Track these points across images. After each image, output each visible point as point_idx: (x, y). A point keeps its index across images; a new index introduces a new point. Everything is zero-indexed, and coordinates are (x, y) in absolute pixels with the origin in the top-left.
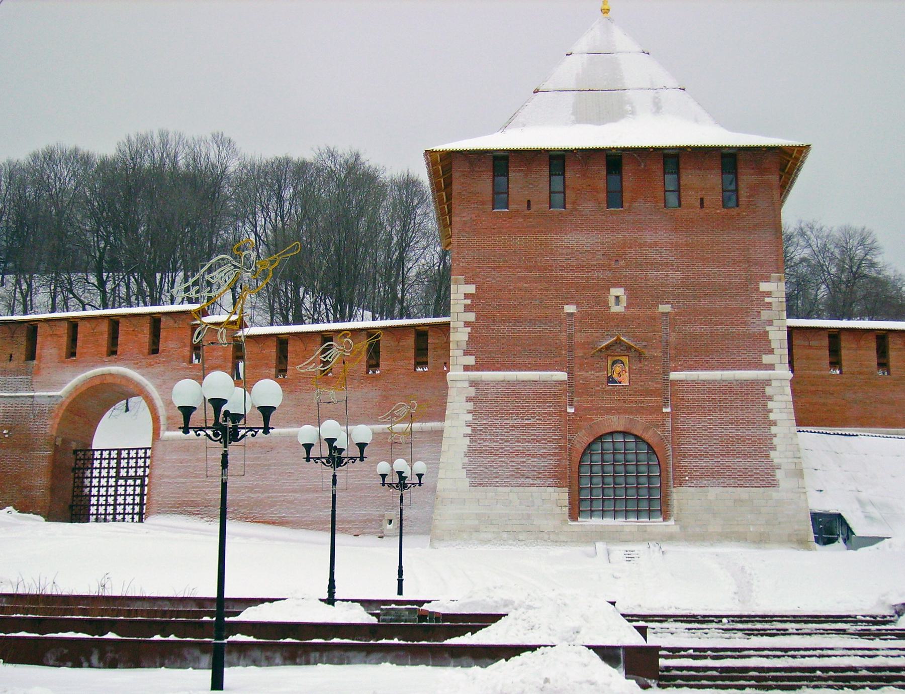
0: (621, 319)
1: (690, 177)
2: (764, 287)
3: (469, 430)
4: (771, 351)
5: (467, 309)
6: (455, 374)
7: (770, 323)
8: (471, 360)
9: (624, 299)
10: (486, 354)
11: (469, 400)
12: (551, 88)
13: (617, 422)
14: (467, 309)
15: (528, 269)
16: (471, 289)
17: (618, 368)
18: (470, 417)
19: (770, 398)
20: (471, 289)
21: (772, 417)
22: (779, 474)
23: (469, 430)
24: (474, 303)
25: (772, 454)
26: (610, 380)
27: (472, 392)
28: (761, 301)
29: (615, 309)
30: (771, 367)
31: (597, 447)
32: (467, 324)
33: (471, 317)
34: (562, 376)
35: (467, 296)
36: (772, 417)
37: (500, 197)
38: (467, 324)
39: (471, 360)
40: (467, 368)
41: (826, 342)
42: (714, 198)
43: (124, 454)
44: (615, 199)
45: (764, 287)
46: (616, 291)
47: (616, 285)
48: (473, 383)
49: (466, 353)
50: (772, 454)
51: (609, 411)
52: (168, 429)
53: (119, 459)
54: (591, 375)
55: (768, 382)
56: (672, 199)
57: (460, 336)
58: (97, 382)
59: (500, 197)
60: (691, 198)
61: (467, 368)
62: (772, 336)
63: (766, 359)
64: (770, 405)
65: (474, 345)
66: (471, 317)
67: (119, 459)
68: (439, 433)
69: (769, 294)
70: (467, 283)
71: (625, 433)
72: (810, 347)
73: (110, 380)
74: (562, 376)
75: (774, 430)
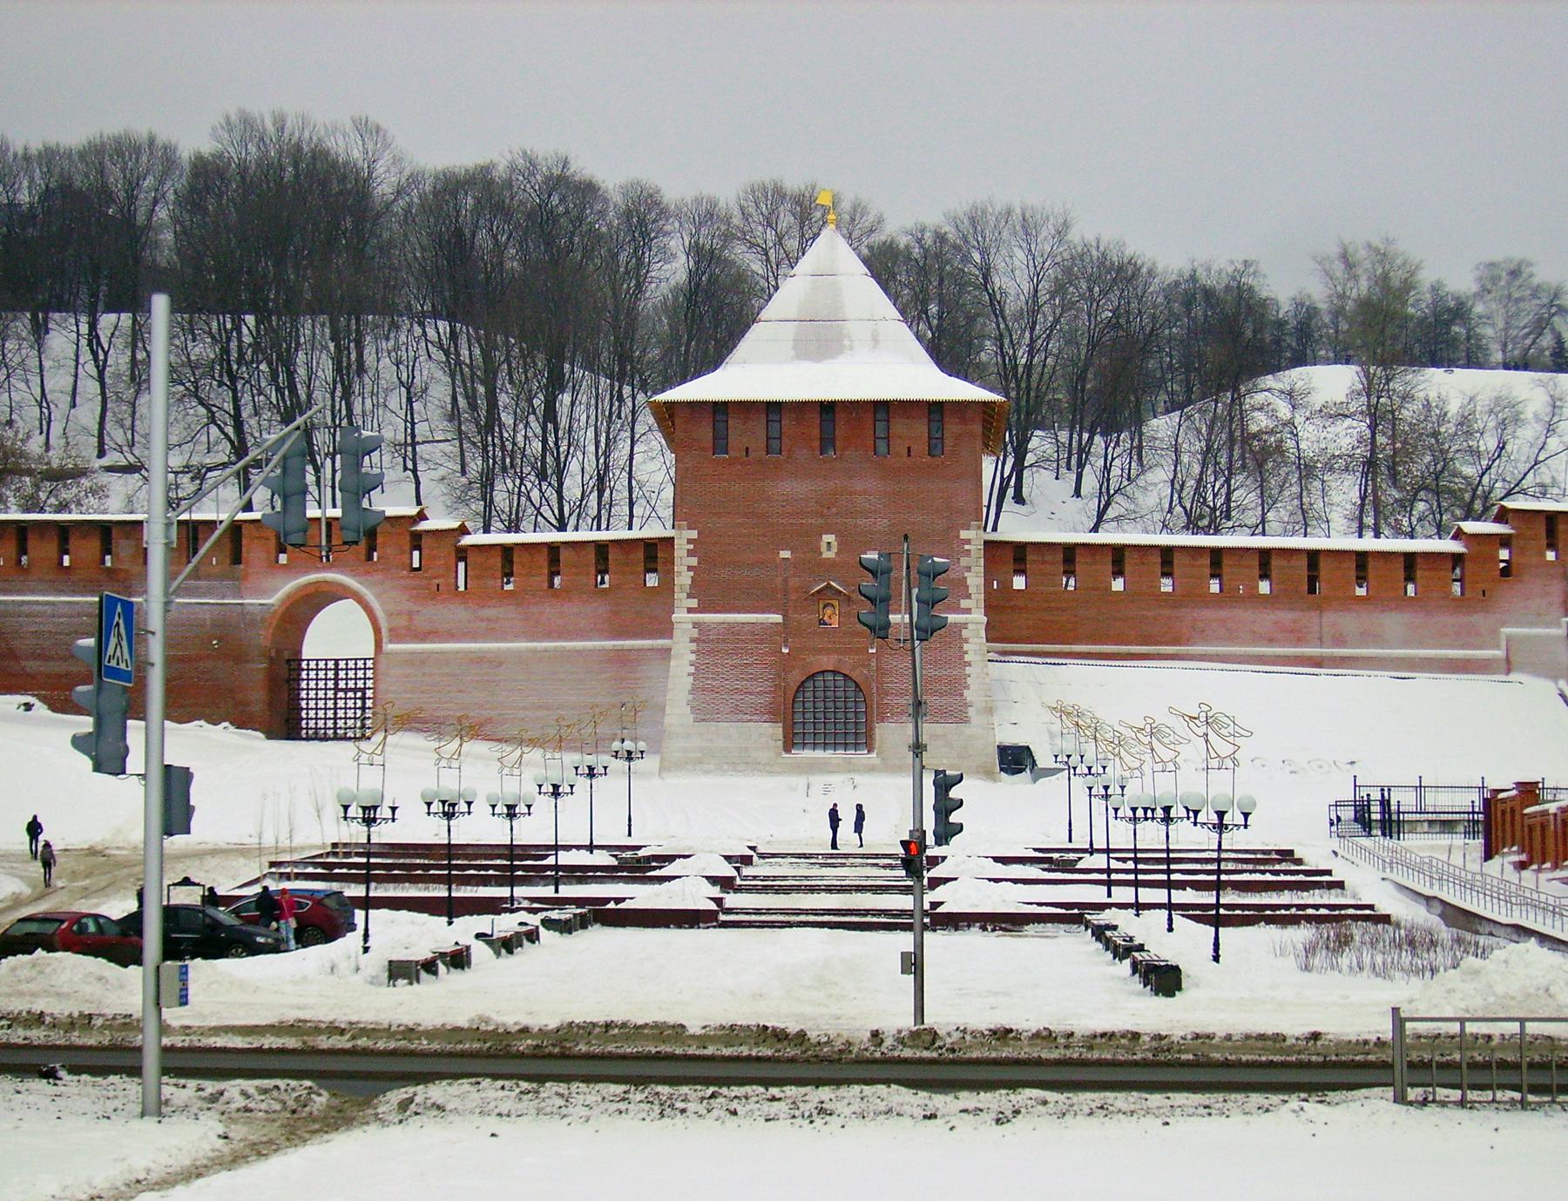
0: (831, 564)
1: (899, 426)
2: (964, 534)
3: (692, 670)
4: (969, 596)
5: (690, 553)
6: (679, 616)
7: (969, 569)
8: (694, 603)
9: (835, 545)
10: (709, 596)
11: (692, 640)
12: (773, 317)
13: (827, 662)
14: (690, 553)
15: (745, 515)
16: (694, 534)
17: (829, 611)
18: (693, 657)
19: (966, 641)
20: (694, 534)
21: (967, 658)
22: (971, 712)
23: (692, 670)
25: (966, 692)
26: (822, 622)
27: (695, 633)
29: (827, 555)
30: (968, 611)
31: (810, 684)
32: (690, 568)
33: (694, 561)
34: (778, 618)
35: (689, 541)
36: (967, 658)
37: (720, 443)
38: (690, 568)
39: (694, 603)
41: (1060, 557)
42: (920, 447)
43: (342, 665)
45: (964, 534)
46: (829, 538)
48: (696, 625)
49: (689, 596)
50: (966, 692)
51: (820, 651)
52: (391, 642)
53: (337, 669)
54: (805, 617)
55: (965, 625)
56: (882, 446)
57: (683, 579)
58: (312, 589)
60: (899, 447)
61: (690, 610)
62: (969, 582)
63: (964, 603)
64: (966, 647)
65: (696, 589)
66: (694, 561)
67: (337, 669)
68: (668, 650)
69: (968, 542)
71: (835, 672)
72: (1044, 562)
73: (325, 588)
74: (778, 618)
75: (968, 670)
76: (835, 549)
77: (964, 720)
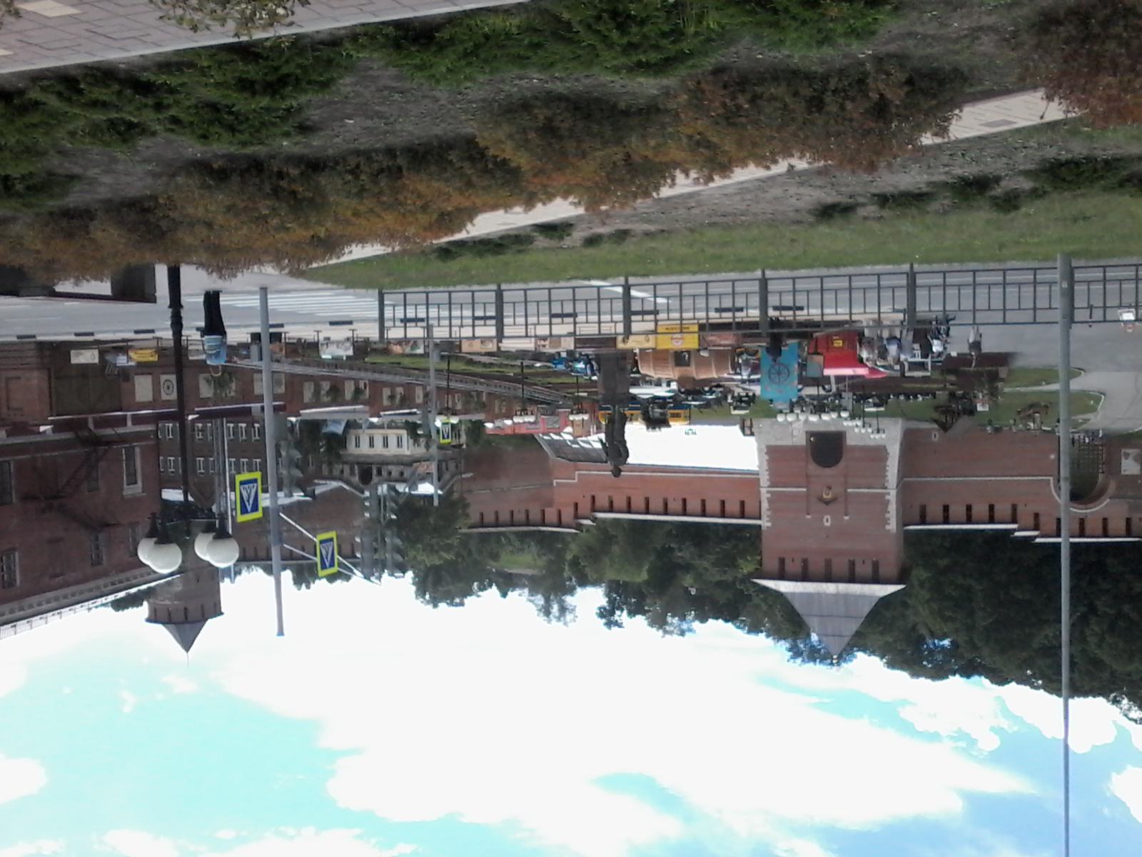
4: (768, 498)
7: (768, 510)
8: (887, 497)
13: (828, 471)
16: (888, 527)
20: (888, 527)
22: (765, 450)
24: (886, 521)
26: (830, 488)
28: (771, 519)
33: (887, 515)
35: (889, 524)
39: (887, 497)
40: (889, 494)
44: (828, 563)
47: (827, 528)
48: (886, 488)
49: (889, 501)
55: (769, 487)
57: (892, 508)
59: (876, 566)
63: (769, 495)
64: (768, 477)
66: (887, 515)
69: (768, 521)
70: (889, 530)
74: (849, 490)
76: (825, 520)
77: (768, 447)
